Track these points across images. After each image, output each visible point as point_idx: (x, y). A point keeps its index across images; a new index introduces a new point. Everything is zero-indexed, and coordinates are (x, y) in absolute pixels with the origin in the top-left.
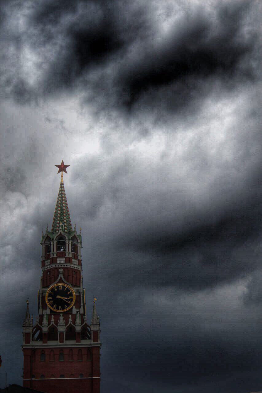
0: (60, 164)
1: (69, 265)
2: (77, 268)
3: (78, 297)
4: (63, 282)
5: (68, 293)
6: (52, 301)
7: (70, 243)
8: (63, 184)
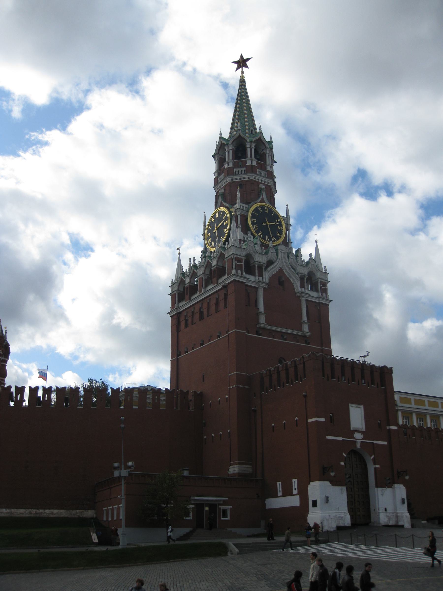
0: (238, 59)
1: (228, 179)
2: (244, 178)
6: (210, 239)
7: (231, 148)
8: (244, 82)
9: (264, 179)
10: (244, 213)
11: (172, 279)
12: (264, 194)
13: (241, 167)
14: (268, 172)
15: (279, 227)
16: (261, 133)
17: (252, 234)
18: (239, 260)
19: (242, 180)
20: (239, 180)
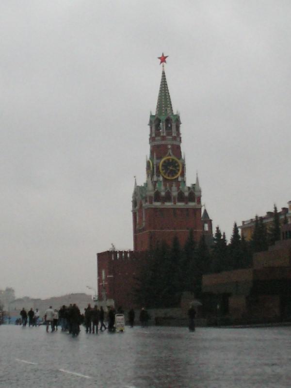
0: (161, 56)
10: (158, 165)
12: (170, 151)
14: (173, 137)
15: (178, 168)
17: (163, 177)
18: (151, 197)
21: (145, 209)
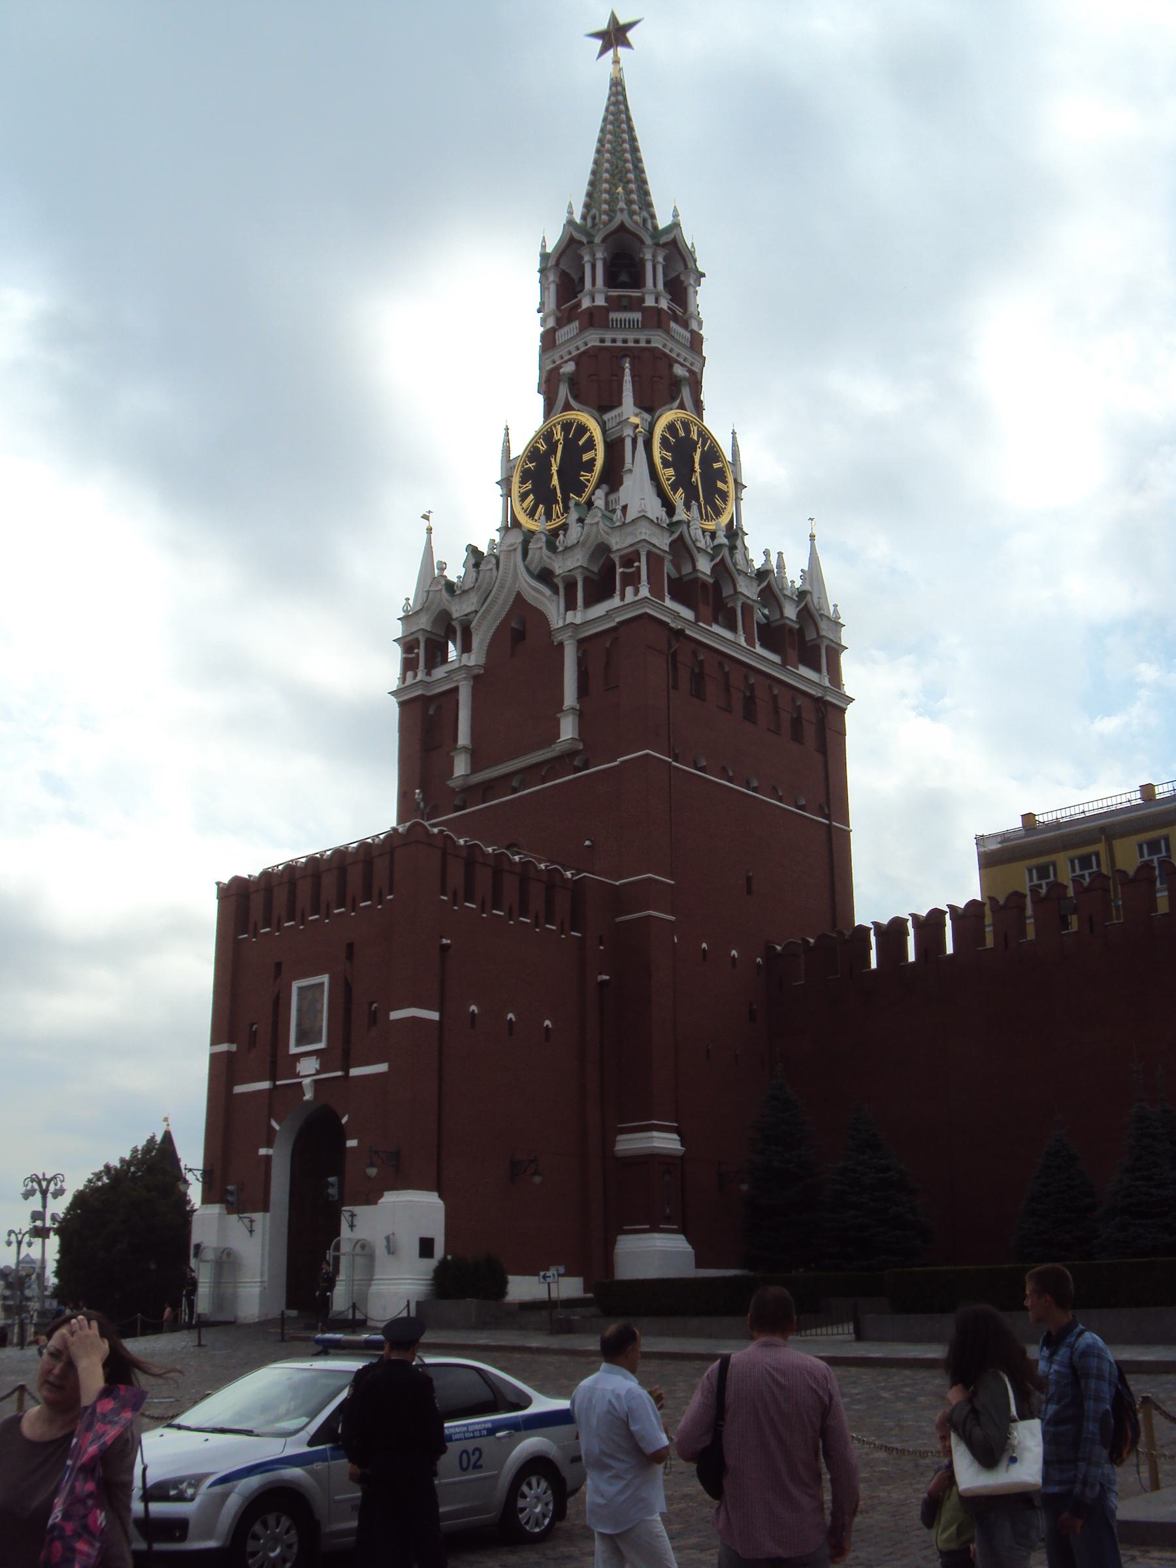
0: (603, 25)
1: (593, 339)
2: (637, 341)
3: (614, 448)
4: (573, 409)
5: (581, 443)
6: (531, 497)
7: (599, 255)
9: (684, 353)
11: (408, 599)
13: (625, 309)
15: (720, 485)
16: (676, 226)
18: (655, 560)
19: (631, 344)
20: (619, 344)
21: (581, 642)
